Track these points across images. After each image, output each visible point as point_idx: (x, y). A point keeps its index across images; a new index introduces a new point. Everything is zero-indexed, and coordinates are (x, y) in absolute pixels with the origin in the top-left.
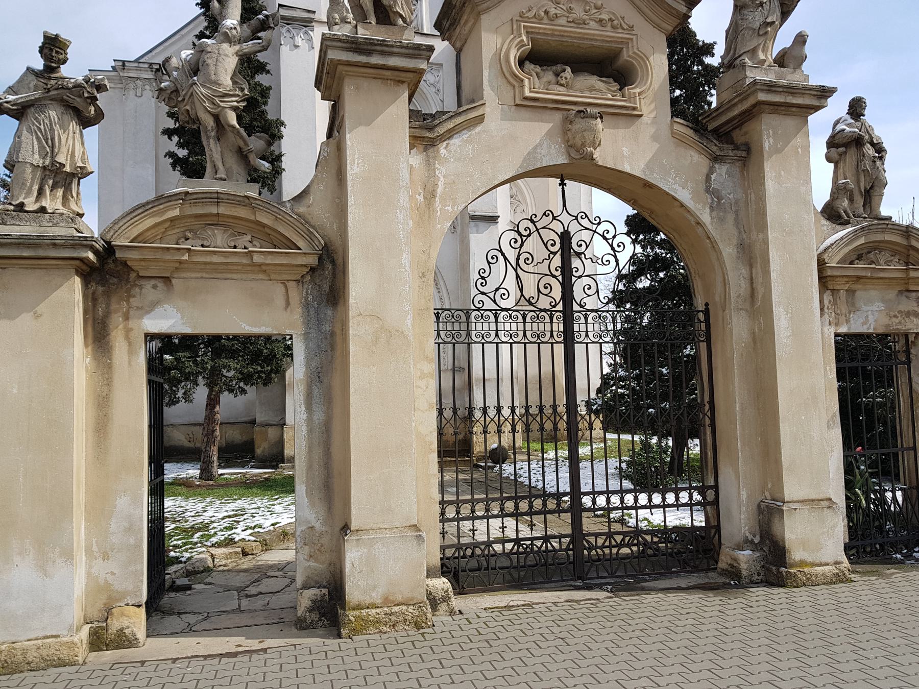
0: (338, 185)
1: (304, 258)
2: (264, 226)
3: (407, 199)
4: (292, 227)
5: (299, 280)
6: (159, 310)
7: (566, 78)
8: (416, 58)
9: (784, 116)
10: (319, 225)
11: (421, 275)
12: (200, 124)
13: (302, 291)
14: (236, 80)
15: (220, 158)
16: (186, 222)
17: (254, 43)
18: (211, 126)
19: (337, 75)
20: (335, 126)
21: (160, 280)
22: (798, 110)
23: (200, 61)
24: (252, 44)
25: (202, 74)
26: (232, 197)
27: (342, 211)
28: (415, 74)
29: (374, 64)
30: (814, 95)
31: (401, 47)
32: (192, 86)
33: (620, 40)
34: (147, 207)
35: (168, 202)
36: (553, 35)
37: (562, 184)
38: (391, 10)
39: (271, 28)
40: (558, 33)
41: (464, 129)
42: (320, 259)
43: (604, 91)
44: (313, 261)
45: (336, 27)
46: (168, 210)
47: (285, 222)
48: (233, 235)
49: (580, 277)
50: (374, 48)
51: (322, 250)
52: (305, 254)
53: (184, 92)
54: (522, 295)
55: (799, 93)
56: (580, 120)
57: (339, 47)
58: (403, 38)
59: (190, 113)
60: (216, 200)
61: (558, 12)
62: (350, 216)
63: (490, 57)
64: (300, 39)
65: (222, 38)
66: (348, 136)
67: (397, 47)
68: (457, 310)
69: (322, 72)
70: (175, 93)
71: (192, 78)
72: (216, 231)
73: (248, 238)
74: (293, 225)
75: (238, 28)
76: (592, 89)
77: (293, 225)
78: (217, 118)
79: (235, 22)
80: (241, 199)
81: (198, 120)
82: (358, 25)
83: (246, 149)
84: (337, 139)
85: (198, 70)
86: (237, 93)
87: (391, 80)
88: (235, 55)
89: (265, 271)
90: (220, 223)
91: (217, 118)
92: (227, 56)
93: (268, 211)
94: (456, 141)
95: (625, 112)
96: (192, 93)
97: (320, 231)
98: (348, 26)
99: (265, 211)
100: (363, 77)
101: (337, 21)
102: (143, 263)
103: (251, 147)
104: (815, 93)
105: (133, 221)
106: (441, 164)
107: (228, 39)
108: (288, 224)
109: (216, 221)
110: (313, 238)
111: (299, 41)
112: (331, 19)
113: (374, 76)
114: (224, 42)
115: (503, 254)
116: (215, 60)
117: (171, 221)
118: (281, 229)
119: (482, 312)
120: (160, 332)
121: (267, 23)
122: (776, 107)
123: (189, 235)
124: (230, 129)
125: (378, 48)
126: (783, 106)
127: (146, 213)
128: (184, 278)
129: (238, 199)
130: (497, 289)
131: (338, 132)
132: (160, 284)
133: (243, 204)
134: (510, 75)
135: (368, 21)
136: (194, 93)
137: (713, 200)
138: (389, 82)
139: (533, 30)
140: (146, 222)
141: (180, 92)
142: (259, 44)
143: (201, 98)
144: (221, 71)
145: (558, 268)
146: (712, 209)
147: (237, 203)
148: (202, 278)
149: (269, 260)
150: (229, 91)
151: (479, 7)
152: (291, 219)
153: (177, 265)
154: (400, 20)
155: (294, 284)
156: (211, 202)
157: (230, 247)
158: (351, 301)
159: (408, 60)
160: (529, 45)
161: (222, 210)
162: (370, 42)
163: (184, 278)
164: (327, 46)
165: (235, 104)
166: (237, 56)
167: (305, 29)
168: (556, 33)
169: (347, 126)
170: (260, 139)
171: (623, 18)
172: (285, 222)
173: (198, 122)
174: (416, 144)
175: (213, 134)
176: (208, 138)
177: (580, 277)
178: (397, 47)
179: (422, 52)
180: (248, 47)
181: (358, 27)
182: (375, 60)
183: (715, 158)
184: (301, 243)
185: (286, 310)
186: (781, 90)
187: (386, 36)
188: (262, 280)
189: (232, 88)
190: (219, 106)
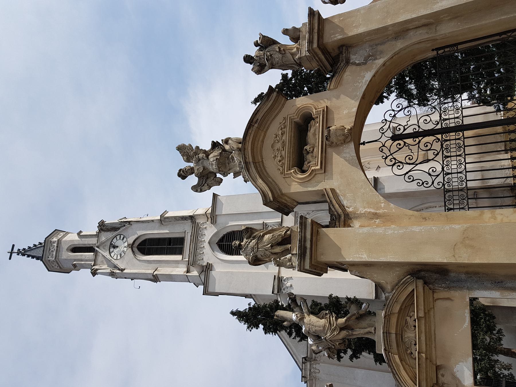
0: (373, 266)
1: (419, 287)
2: (401, 309)
3: (380, 229)
4: (401, 293)
5: (433, 291)
6: (458, 375)
7: (310, 148)
8: (306, 224)
9: (324, 31)
10: (397, 278)
11: (424, 220)
12: (345, 338)
13: (439, 290)
14: (321, 317)
15: (363, 330)
16: (402, 352)
17: (303, 306)
18: (346, 332)
19: (316, 264)
20: (341, 267)
21: (438, 372)
23: (314, 334)
24: (303, 307)
25: (320, 334)
26: (386, 325)
27: (388, 265)
28: (313, 224)
29: (310, 245)
30: (313, 18)
31: (301, 232)
32: (326, 340)
34: (395, 373)
35: (391, 361)
36: (290, 157)
37: (364, 143)
38: (283, 237)
39: (295, 297)
40: (289, 154)
41: (339, 199)
42: (418, 278)
43: (315, 128)
44: (420, 283)
45: (293, 264)
46: (396, 361)
47: (398, 297)
48: (407, 327)
49: (419, 127)
50: (303, 246)
51: (414, 277)
52: (416, 287)
53: (330, 345)
54: (433, 159)
55: (313, 26)
56: (331, 138)
57: (304, 263)
58: (296, 231)
59: (340, 342)
60: (388, 334)
61: (279, 155)
62: (392, 260)
63: (302, 187)
64: (288, 284)
65: (302, 322)
66: (347, 260)
67: (302, 234)
68: (445, 198)
69: (315, 272)
70: (330, 349)
71: (322, 340)
72: (406, 336)
73: (408, 318)
74: (400, 292)
75: (297, 313)
76: (314, 134)
77: (400, 292)
78: (342, 329)
79: (294, 314)
80: (386, 320)
81: (343, 339)
82: (292, 253)
83: (357, 315)
84: (348, 266)
85: (318, 336)
86: (328, 317)
87: (317, 237)
88: (309, 316)
89: (428, 311)
90: (401, 333)
91: (342, 329)
92: (310, 320)
93: (392, 306)
94: (345, 203)
95: (325, 116)
96: (330, 340)
97: (401, 278)
98: (292, 258)
99: (392, 308)
100: (316, 251)
101: (290, 263)
102: (429, 380)
103: (355, 312)
104: (312, 18)
105: (403, 382)
106: (358, 210)
107: (302, 319)
108: (399, 295)
109: (400, 335)
110: (406, 282)
111: (288, 284)
112: (290, 266)
113: (316, 246)
114: (304, 321)
115: (407, 173)
116: (313, 326)
117: (401, 360)
118: (402, 299)
119: (445, 183)
120: (472, 376)
121: (293, 298)
122: (320, 36)
123: (409, 351)
124: (347, 322)
125: (303, 243)
126: (319, 33)
127: (398, 374)
128: (436, 357)
129: (386, 322)
130: (430, 174)
131: (344, 265)
132: (441, 372)
133: (389, 319)
134: (310, 177)
135: (290, 248)
136: (330, 339)
137: (370, 60)
138: (318, 238)
139: (288, 167)
140: (403, 374)
141: (329, 346)
142: (303, 303)
143: (333, 336)
144: (317, 324)
145: (414, 140)
146: (376, 59)
147: (388, 322)
148: (435, 347)
149: (422, 307)
150: (328, 321)
151: (280, 194)
152: (396, 293)
153: (428, 361)
154: (288, 232)
155: (435, 294)
156: (389, 337)
157: (415, 329)
158: (445, 261)
159: (307, 228)
160: (295, 168)
161: (393, 331)
162: (300, 247)
163: (436, 357)
164: (303, 269)
165: (334, 318)
166: (310, 315)
167: (283, 281)
169: (342, 260)
170: (351, 307)
171: (280, 123)
172: (398, 297)
173: (344, 339)
174: (348, 224)
175: (350, 332)
176: (353, 335)
177: (419, 127)
178: (302, 234)
179: (303, 222)
180: (305, 310)
181: (293, 253)
182: (308, 245)
184: (410, 289)
185: (453, 300)
186: (311, 36)
187: (296, 239)
188: (434, 313)
189: (326, 319)
190: (336, 327)
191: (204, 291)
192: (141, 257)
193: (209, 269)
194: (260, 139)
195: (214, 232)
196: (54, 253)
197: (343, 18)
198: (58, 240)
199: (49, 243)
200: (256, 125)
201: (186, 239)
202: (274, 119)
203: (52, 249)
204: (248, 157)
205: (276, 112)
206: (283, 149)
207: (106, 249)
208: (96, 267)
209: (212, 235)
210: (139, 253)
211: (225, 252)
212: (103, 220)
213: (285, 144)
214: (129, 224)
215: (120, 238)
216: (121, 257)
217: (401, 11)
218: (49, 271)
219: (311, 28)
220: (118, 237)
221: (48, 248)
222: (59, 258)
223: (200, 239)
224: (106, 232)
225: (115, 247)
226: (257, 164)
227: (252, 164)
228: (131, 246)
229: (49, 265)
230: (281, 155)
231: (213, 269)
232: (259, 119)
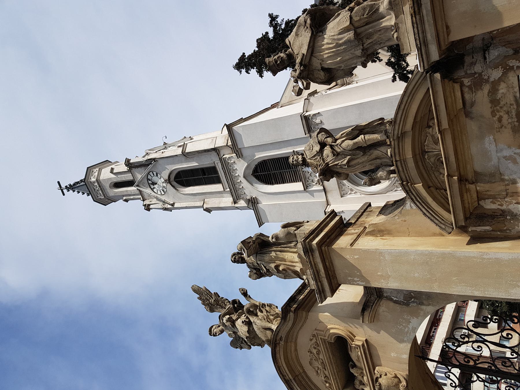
9: (334, 266)
22: (327, 261)
30: (313, 257)
33: (324, 343)
36: (336, 379)
55: (316, 267)
95: (367, 352)
104: (311, 257)
122: (331, 277)
126: (329, 273)
137: (413, 302)
146: (422, 304)
168: (334, 378)
183: (379, 298)
186: (319, 284)
191: (259, 224)
192: (183, 189)
193: (255, 203)
194: (292, 350)
195: (244, 166)
196: (101, 192)
197: (358, 257)
198: (97, 180)
199: (90, 183)
200: (282, 343)
201: (217, 166)
202: (300, 328)
203: (96, 189)
204: (285, 373)
205: (300, 325)
206: (325, 370)
207: (146, 186)
208: (147, 202)
209: (244, 168)
210: (180, 186)
211: (264, 182)
212: (128, 158)
213: (325, 364)
214: (155, 161)
215: (154, 175)
216: (164, 192)
217: (454, 278)
218: (105, 205)
219: (315, 271)
220: (151, 173)
221: (92, 188)
222: (108, 195)
223: (233, 174)
224: (136, 169)
225: (154, 184)
226: (300, 377)
227: (293, 381)
228: (168, 181)
229: (102, 202)
230: (325, 376)
231: (259, 202)
232: (282, 336)
